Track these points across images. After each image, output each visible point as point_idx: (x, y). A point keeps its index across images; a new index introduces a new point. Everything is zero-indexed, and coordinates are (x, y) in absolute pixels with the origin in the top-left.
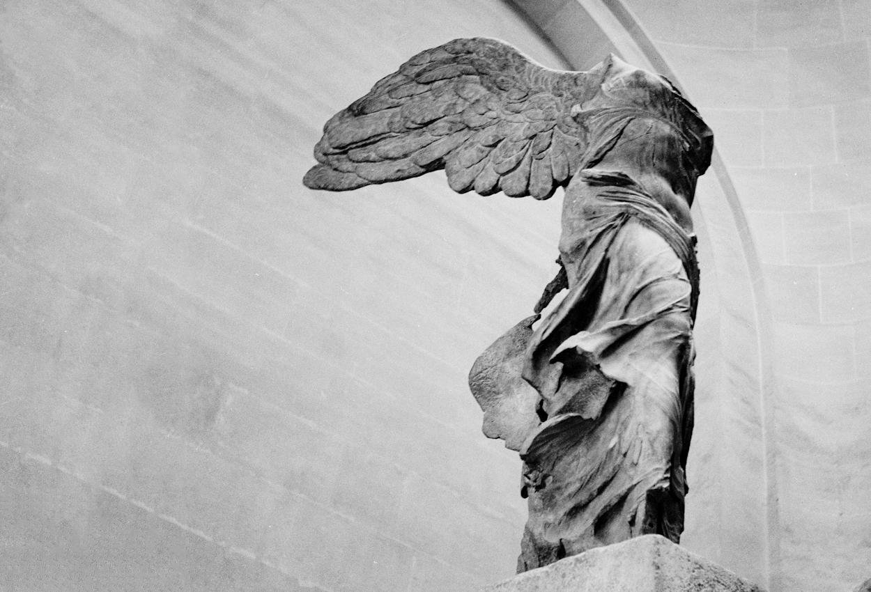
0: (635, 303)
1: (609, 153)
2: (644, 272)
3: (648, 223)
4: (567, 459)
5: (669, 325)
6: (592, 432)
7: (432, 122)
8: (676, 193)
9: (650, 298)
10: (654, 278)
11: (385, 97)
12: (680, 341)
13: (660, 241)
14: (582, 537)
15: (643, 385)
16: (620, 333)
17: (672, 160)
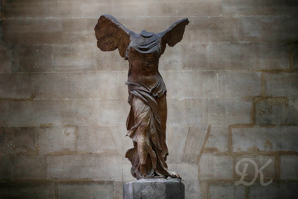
0: (137, 120)
1: (131, 71)
2: (136, 113)
3: (137, 97)
4: (134, 155)
5: (141, 126)
6: (136, 150)
7: (112, 34)
8: (148, 76)
9: (138, 120)
10: (138, 114)
11: (101, 25)
12: (144, 129)
13: (140, 101)
14: (137, 172)
15: (138, 142)
16: (134, 130)
17: (144, 69)
